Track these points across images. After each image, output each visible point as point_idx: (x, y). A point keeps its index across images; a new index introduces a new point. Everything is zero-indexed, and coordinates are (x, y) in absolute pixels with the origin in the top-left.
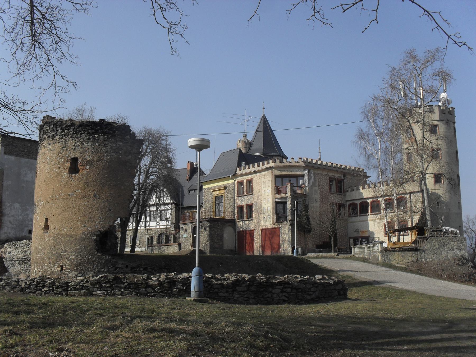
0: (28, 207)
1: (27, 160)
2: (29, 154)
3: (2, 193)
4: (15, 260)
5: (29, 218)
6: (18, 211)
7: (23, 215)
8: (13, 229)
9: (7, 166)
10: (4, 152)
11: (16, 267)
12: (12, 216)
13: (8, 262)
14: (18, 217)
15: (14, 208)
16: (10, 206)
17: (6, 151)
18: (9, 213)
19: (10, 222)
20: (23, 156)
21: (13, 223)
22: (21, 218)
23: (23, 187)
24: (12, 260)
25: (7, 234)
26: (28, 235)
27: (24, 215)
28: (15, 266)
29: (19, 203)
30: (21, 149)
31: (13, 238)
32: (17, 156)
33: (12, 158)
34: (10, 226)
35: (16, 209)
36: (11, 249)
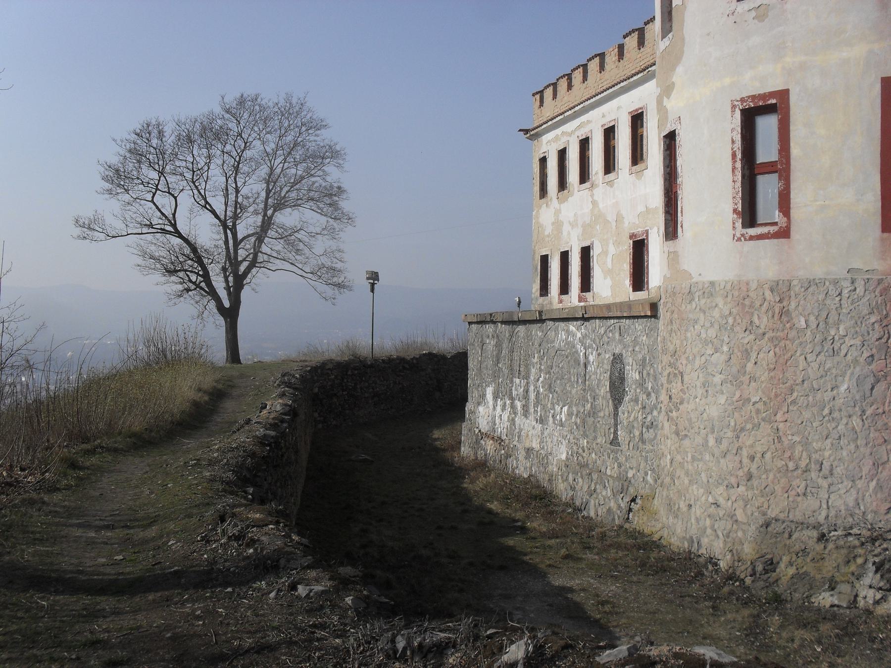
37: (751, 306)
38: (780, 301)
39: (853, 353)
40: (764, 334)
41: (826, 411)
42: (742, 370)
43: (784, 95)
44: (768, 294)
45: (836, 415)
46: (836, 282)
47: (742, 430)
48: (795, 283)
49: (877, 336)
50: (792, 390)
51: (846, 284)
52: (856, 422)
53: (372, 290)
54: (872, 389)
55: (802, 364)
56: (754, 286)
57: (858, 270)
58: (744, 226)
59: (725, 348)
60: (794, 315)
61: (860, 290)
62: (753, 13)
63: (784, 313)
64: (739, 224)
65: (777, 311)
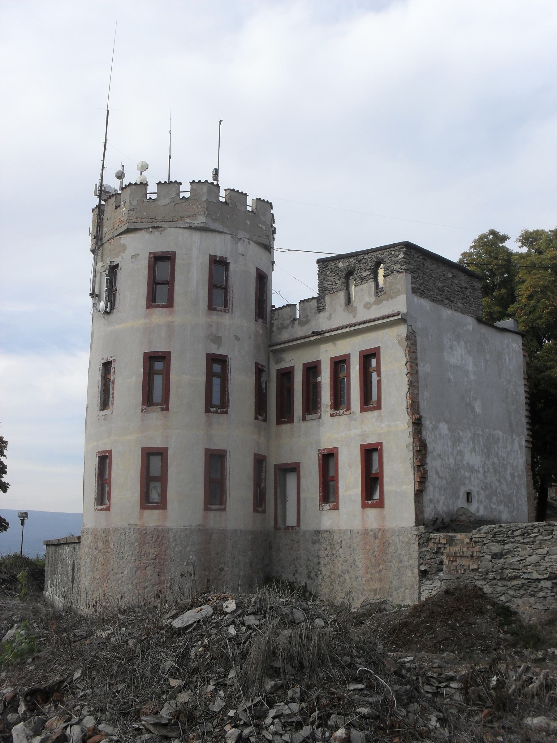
0: (461, 433)
1: (450, 312)
2: (451, 299)
3: (418, 394)
4: (535, 576)
5: (464, 463)
6: (447, 445)
7: (455, 453)
8: (443, 492)
9: (420, 326)
10: (412, 289)
11: (545, 598)
12: (439, 455)
13: (495, 582)
14: (448, 459)
15: (440, 434)
16: (433, 430)
17: (414, 285)
18: (434, 448)
19: (437, 473)
20: (440, 302)
21: (441, 475)
22: (452, 460)
23: (449, 380)
24: (516, 578)
25: (434, 503)
26: (465, 505)
27: (457, 454)
28: (541, 594)
29: (447, 422)
30: (440, 284)
31: (445, 516)
32: (433, 301)
33: (426, 304)
34: (437, 482)
35: (443, 438)
36: (507, 547)
37: (97, 539)
38: (106, 537)
39: (129, 558)
40: (100, 550)
41: (120, 582)
42: (94, 566)
43: (110, 452)
44: (102, 533)
45: (123, 584)
46: (124, 529)
47: (94, 591)
48: (111, 529)
49: (137, 552)
50: (109, 573)
51: (127, 530)
52: (130, 586)
53: (22, 524)
54: (135, 573)
55: (112, 562)
56: (99, 530)
57: (132, 524)
58: (97, 505)
59: (90, 557)
60: (110, 542)
61: (132, 532)
62: (103, 417)
63: (107, 541)
64: (96, 504)
65: (105, 540)
